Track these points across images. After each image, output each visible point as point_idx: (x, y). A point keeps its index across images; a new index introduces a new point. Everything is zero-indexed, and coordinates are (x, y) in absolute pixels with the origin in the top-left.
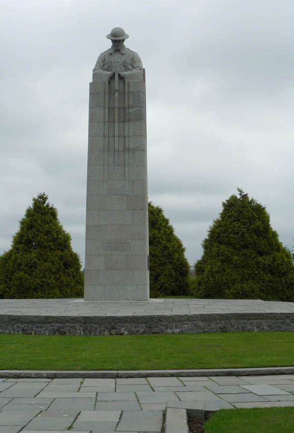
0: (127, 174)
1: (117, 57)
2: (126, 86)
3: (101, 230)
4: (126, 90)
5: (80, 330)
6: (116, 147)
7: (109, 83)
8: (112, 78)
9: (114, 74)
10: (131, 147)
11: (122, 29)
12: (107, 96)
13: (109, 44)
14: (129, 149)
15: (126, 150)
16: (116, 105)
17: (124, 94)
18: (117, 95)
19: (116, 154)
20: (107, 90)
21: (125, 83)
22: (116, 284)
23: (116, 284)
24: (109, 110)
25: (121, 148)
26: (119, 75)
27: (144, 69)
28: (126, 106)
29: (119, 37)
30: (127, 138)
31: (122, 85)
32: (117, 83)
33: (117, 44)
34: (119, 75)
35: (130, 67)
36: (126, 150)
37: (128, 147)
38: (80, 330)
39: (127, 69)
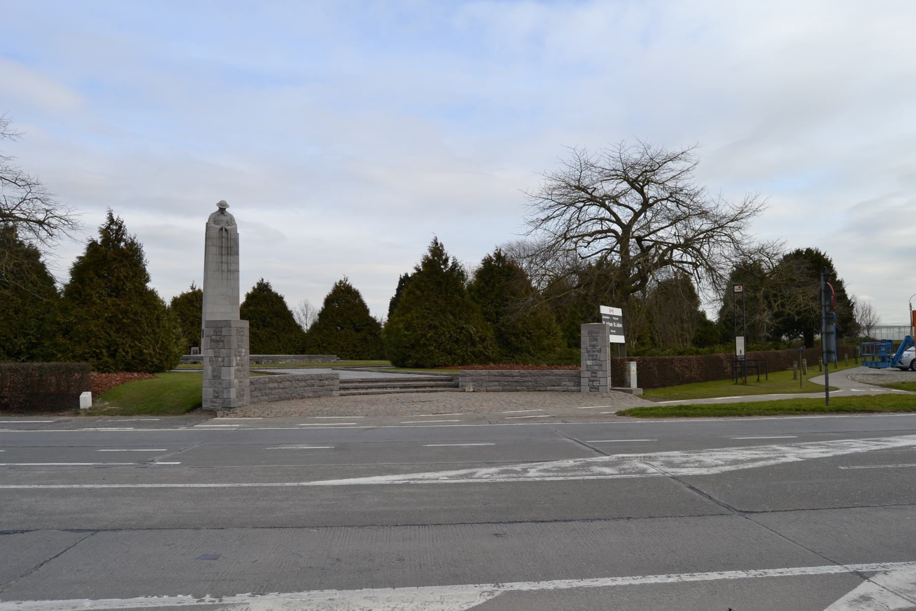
1: (223, 217)
4: (229, 237)
6: (223, 269)
8: (222, 229)
9: (222, 228)
10: (231, 269)
11: (226, 202)
13: (217, 209)
15: (229, 271)
16: (223, 245)
17: (231, 239)
18: (224, 240)
19: (223, 273)
21: (228, 233)
25: (226, 270)
26: (225, 229)
28: (229, 246)
30: (229, 265)
31: (226, 234)
32: (224, 234)
34: (225, 229)
35: (230, 224)
36: (229, 271)
39: (229, 225)
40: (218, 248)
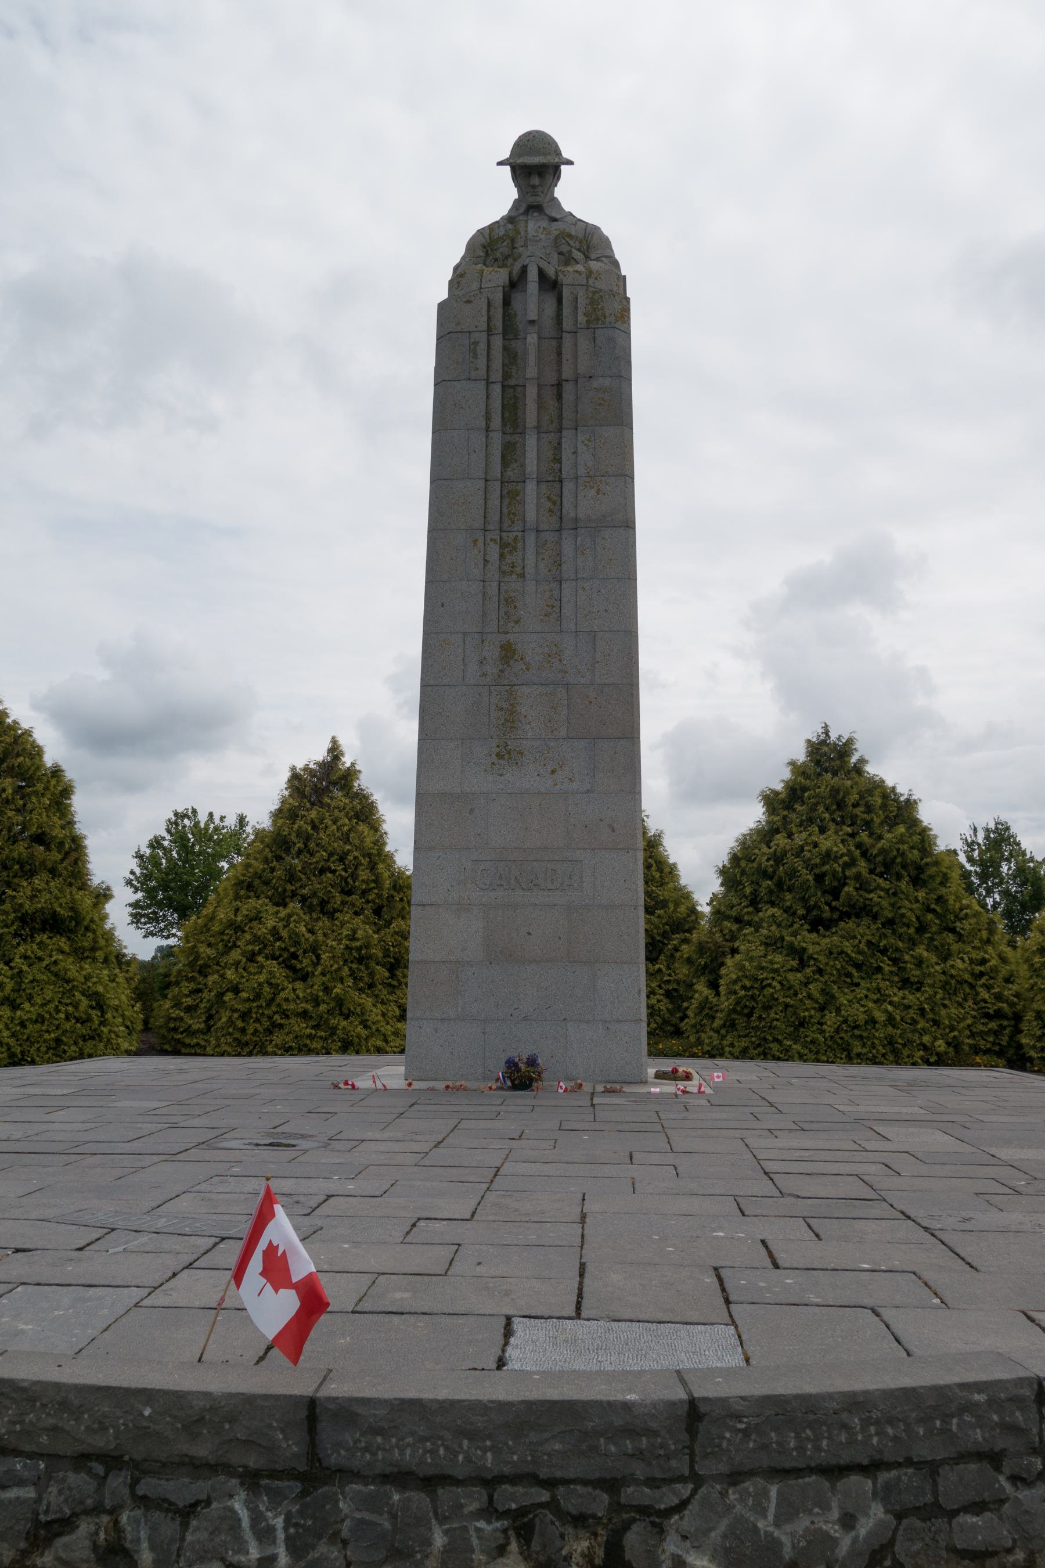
0: (568, 610)
1: (533, 226)
2: (566, 311)
3: (472, 811)
5: (265, 1535)
7: (507, 302)
8: (516, 284)
9: (524, 270)
10: (581, 515)
12: (498, 342)
14: (576, 520)
16: (531, 371)
18: (532, 339)
20: (498, 323)
22: (525, 1018)
23: (525, 1018)
24: (503, 391)
27: (624, 277)
28: (567, 373)
29: (545, 155)
30: (568, 487)
33: (535, 180)
34: (541, 273)
37: (573, 515)
38: (265, 1535)
40: (497, 390)
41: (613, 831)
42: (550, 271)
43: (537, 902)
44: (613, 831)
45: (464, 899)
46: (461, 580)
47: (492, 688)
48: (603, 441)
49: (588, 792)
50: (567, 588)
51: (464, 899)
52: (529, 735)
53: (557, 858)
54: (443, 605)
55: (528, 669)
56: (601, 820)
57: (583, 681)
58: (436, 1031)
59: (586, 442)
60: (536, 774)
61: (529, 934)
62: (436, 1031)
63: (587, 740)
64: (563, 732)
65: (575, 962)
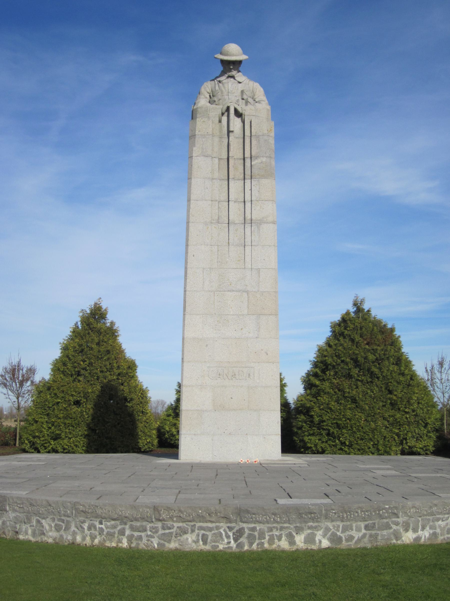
0: (248, 259)
3: (207, 346)
23: (230, 434)
41: (267, 354)
42: (239, 109)
43: (235, 385)
44: (267, 354)
45: (203, 383)
46: (201, 245)
47: (215, 292)
48: (263, 185)
49: (257, 338)
50: (248, 249)
51: (203, 383)
52: (231, 313)
53: (243, 366)
54: (194, 256)
55: (231, 285)
56: (262, 350)
57: (254, 290)
58: (192, 439)
59: (255, 185)
60: (234, 330)
61: (232, 398)
62: (192, 439)
63: (256, 316)
64: (246, 312)
65: (251, 410)
